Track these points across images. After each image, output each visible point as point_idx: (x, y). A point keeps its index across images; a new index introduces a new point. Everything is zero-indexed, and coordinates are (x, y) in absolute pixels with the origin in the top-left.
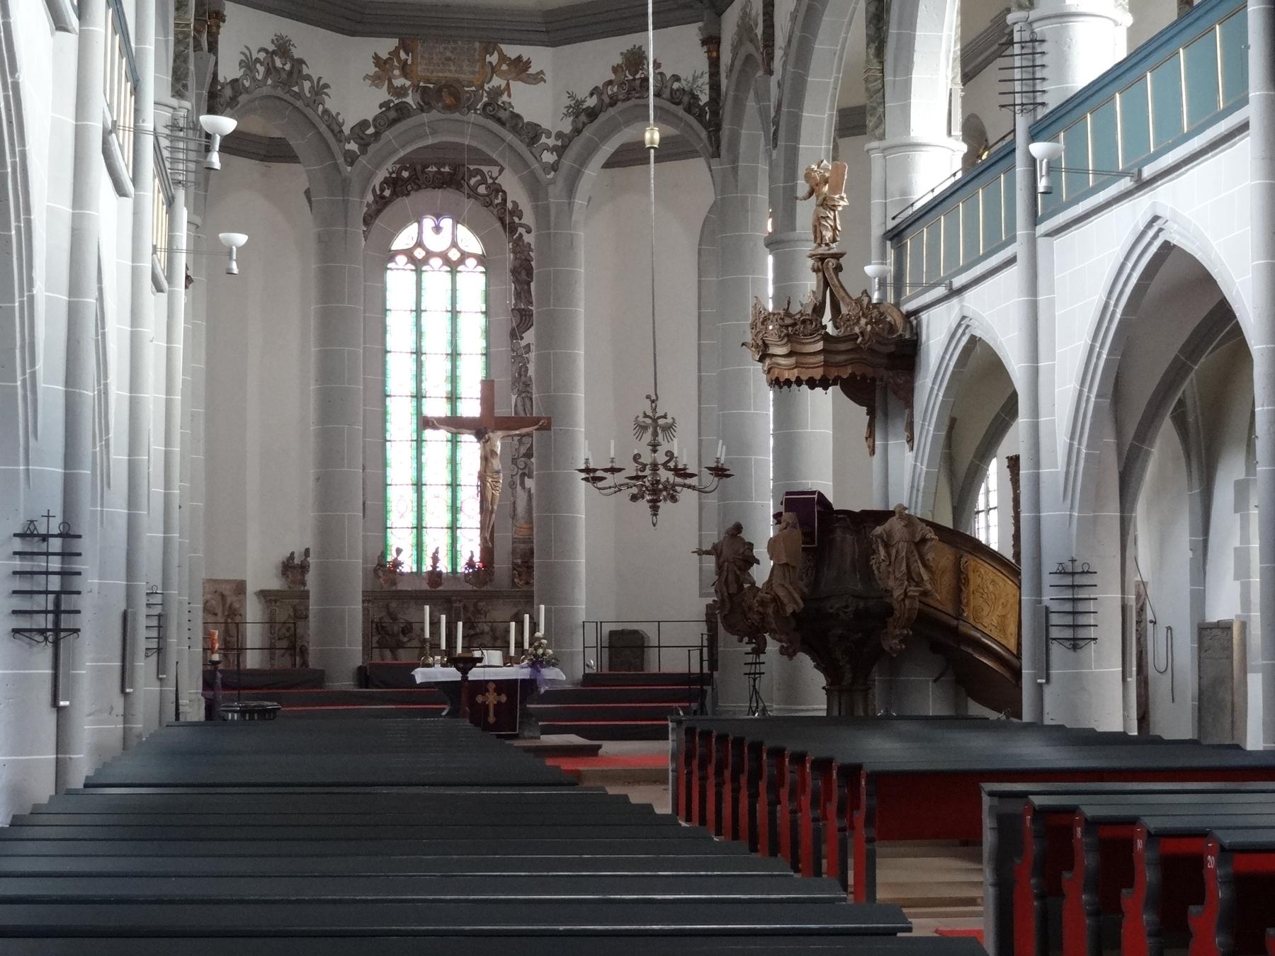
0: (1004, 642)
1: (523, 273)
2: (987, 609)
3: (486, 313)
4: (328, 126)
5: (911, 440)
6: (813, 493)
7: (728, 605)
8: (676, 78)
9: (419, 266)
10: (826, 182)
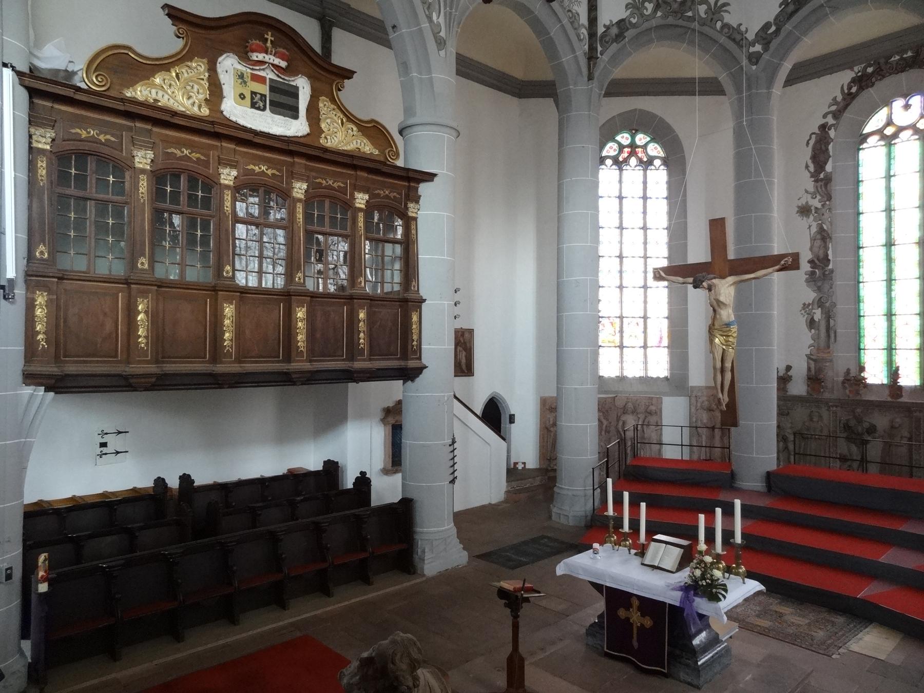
4: (729, 37)
9: (889, 141)
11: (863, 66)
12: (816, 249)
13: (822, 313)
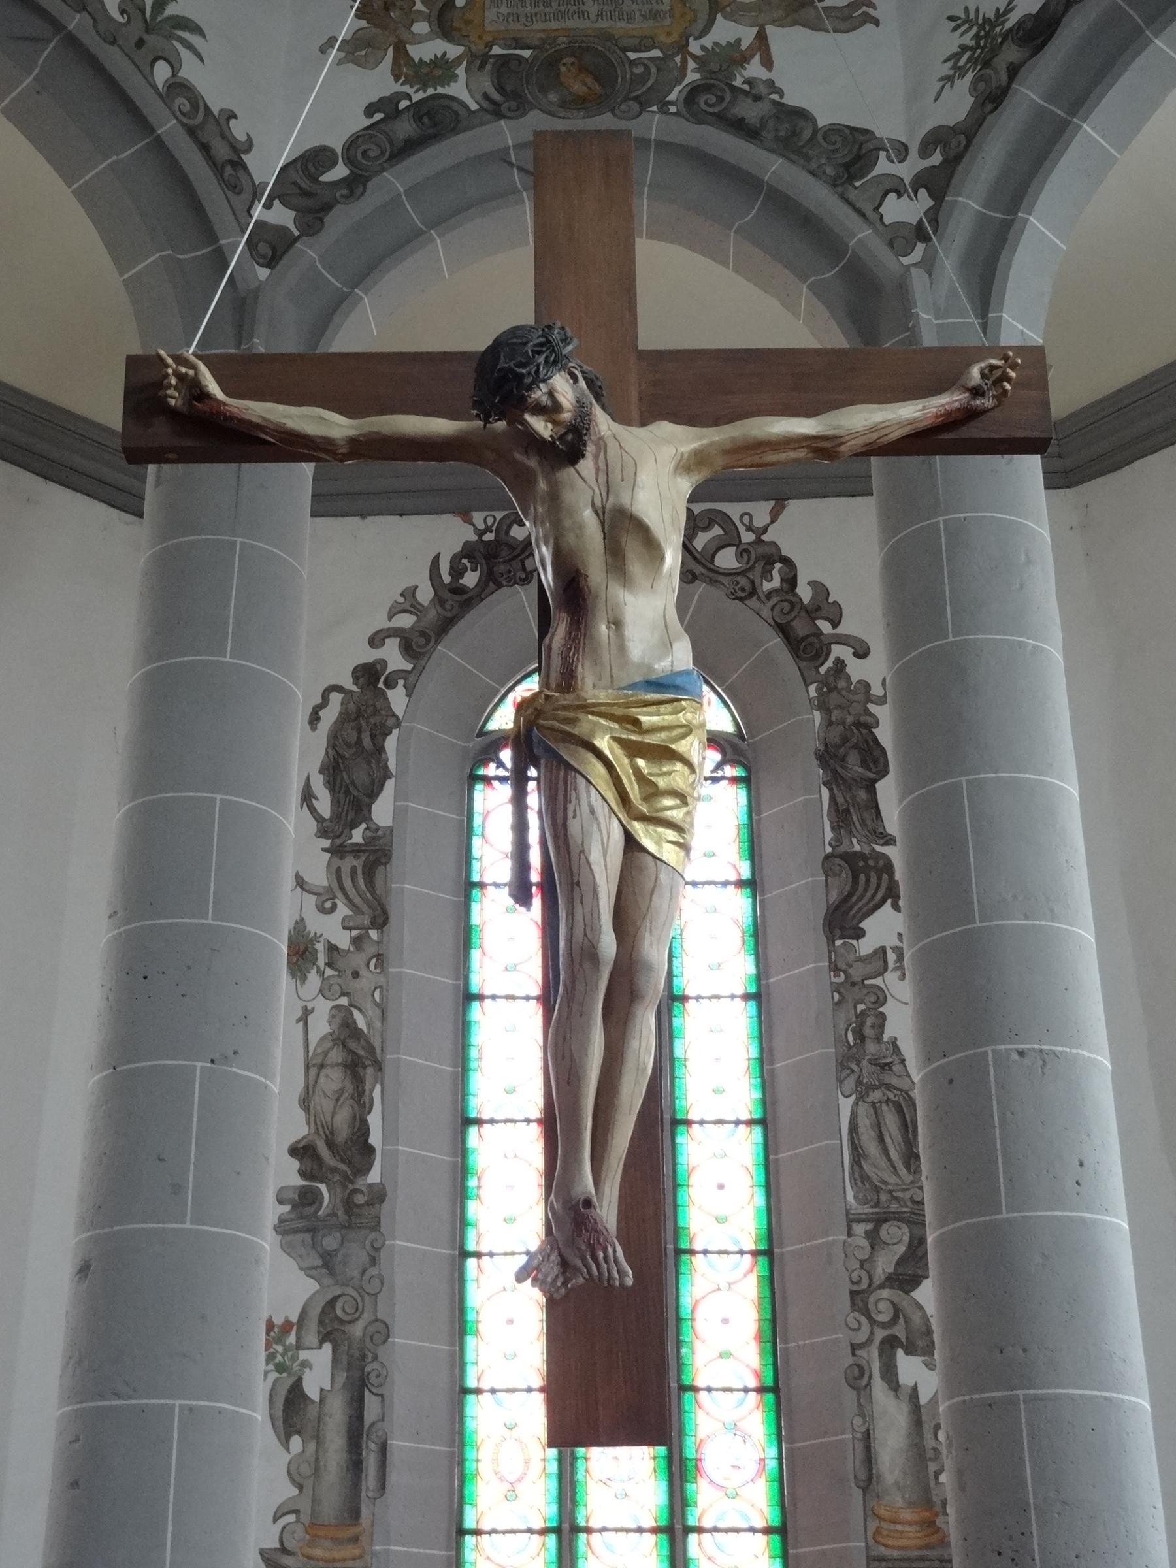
1: (853, 759)
3: (752, 885)
4: (191, 131)
11: (499, 515)
12: (323, 1104)
13: (335, 1361)
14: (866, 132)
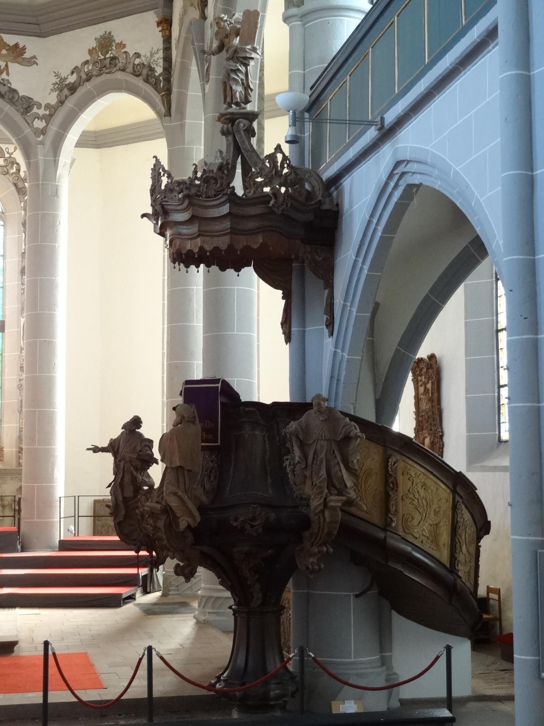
0: (436, 554)
2: (417, 517)
5: (330, 324)
6: (216, 381)
7: (123, 512)
8: (138, 55)
10: (237, 34)
14: (31, 99)
